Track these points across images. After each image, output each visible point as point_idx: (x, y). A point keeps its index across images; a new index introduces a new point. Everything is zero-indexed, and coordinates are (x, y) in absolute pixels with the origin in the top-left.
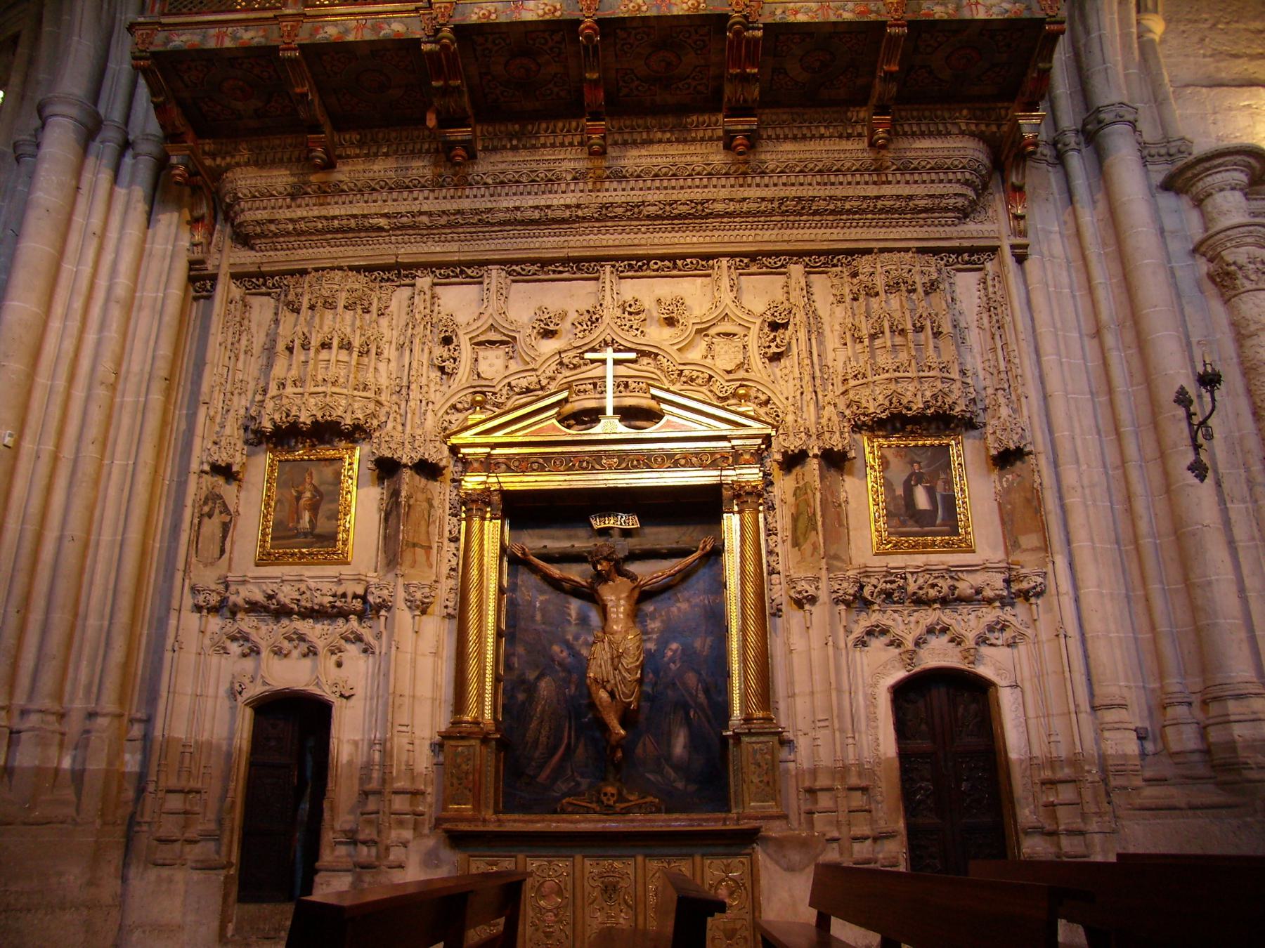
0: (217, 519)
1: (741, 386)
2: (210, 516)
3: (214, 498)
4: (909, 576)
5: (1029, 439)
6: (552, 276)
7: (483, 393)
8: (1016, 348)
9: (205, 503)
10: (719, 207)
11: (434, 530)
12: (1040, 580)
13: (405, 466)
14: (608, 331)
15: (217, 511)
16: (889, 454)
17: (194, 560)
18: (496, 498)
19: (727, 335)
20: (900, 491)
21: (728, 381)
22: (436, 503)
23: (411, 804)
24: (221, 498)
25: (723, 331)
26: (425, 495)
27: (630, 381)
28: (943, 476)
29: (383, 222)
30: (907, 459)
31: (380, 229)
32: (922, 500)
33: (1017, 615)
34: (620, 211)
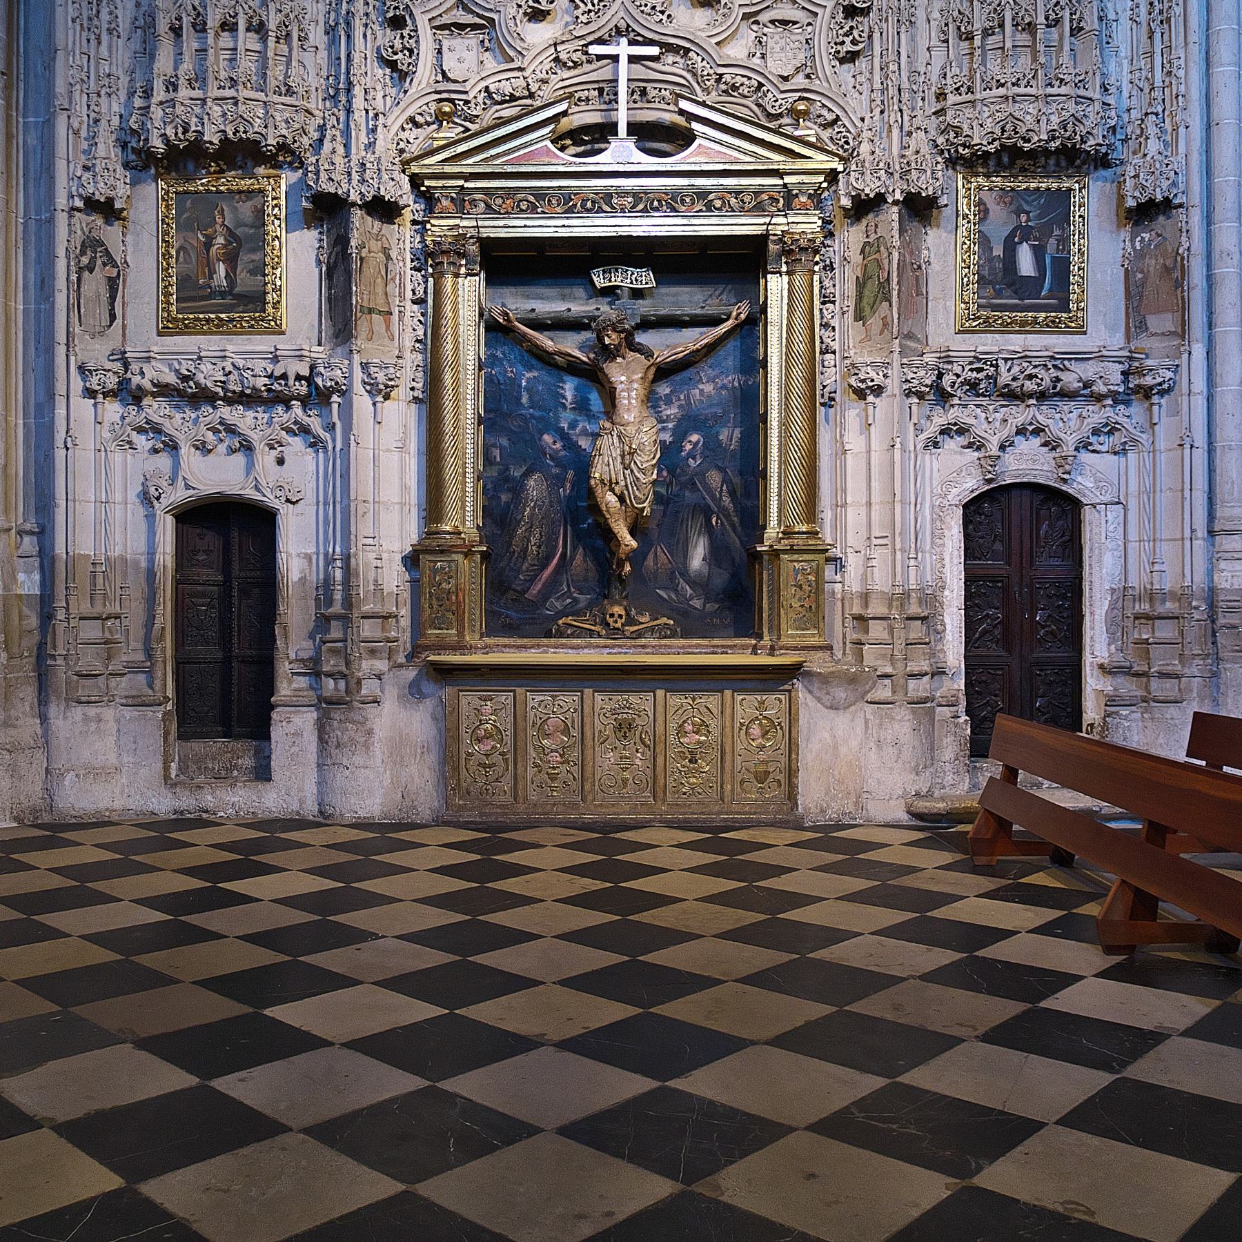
1: (801, 99)
3: (92, 244)
4: (1001, 363)
5: (1182, 187)
7: (452, 101)
8: (1182, 56)
9: (83, 253)
11: (393, 289)
12: (1169, 374)
13: (354, 204)
14: (622, 14)
15: (99, 262)
16: (989, 199)
17: (77, 330)
18: (473, 249)
19: (784, 23)
20: (998, 251)
21: (782, 92)
22: (394, 254)
24: (103, 244)
25: (780, 18)
27: (649, 86)
28: (1057, 232)
30: (1013, 207)
32: (1026, 264)
33: (1131, 416)
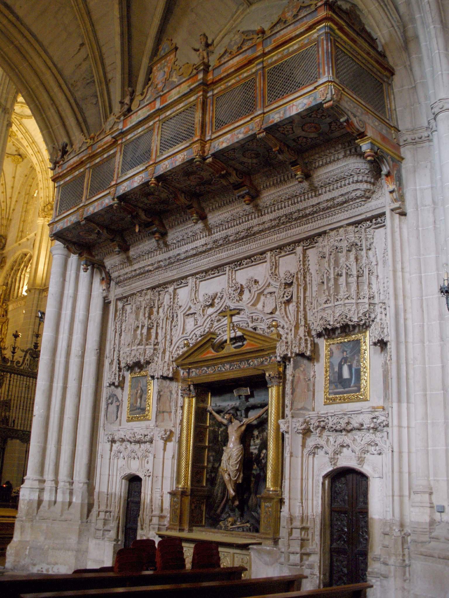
0: (115, 404)
1: (273, 320)
2: (112, 403)
3: (113, 396)
4: (330, 418)
5: (386, 333)
6: (212, 276)
7: (187, 339)
9: (109, 399)
10: (256, 229)
11: (173, 404)
12: (384, 418)
15: (114, 401)
16: (333, 347)
17: (106, 422)
19: (271, 293)
20: (336, 369)
23: (159, 521)
24: (115, 395)
26: (168, 390)
27: (240, 323)
28: (356, 358)
29: (150, 268)
30: (341, 350)
31: (151, 271)
32: (346, 375)
33: (377, 437)
34: (221, 242)
